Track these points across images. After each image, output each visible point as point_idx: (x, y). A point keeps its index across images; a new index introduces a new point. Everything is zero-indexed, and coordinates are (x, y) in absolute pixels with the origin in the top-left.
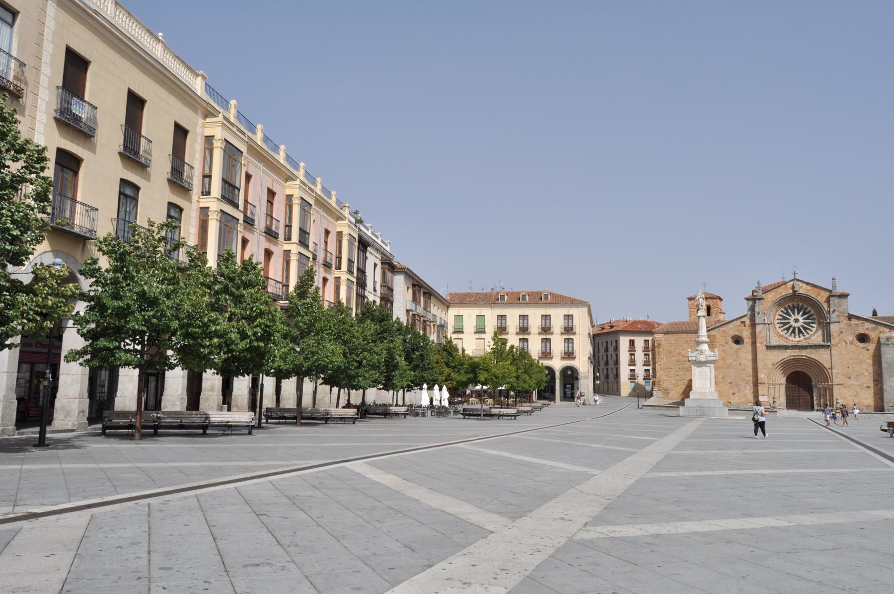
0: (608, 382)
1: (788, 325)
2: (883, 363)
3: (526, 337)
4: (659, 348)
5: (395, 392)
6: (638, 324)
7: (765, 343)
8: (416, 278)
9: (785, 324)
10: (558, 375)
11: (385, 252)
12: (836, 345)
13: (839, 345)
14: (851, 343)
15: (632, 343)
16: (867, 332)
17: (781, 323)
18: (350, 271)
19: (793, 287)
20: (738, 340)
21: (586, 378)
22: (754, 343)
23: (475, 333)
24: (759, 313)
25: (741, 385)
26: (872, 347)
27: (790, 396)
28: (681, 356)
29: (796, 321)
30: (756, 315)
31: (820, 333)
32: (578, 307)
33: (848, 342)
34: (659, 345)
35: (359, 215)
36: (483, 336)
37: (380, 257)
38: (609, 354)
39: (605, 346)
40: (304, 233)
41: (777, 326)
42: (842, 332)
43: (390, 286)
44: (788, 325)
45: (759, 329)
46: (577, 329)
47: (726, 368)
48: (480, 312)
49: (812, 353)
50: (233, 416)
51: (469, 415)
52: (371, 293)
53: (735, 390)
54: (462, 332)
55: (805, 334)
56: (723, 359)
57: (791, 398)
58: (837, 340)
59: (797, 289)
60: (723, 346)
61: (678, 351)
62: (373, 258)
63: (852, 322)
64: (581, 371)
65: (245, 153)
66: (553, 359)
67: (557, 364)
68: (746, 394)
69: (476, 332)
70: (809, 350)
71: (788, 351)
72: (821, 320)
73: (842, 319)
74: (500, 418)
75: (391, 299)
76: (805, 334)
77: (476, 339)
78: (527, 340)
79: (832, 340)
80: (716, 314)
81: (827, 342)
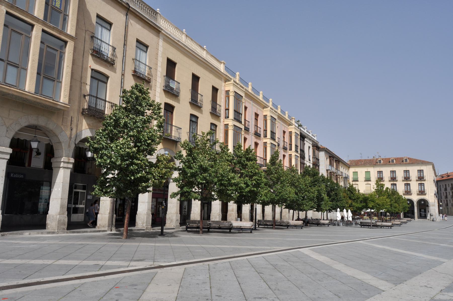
0: (448, 208)
3: (395, 183)
5: (323, 213)
8: (331, 153)
10: (415, 204)
11: (314, 140)
18: (296, 151)
21: (434, 205)
23: (365, 181)
32: (426, 165)
35: (300, 123)
36: (369, 182)
37: (311, 143)
38: (448, 192)
39: (444, 187)
40: (273, 133)
43: (317, 158)
46: (426, 178)
48: (367, 170)
50: (243, 224)
51: (364, 225)
52: (308, 162)
54: (357, 181)
62: (308, 144)
64: (430, 201)
65: (244, 97)
66: (412, 195)
67: (415, 198)
69: (365, 181)
74: (382, 227)
75: (318, 164)
77: (366, 184)
78: (395, 184)
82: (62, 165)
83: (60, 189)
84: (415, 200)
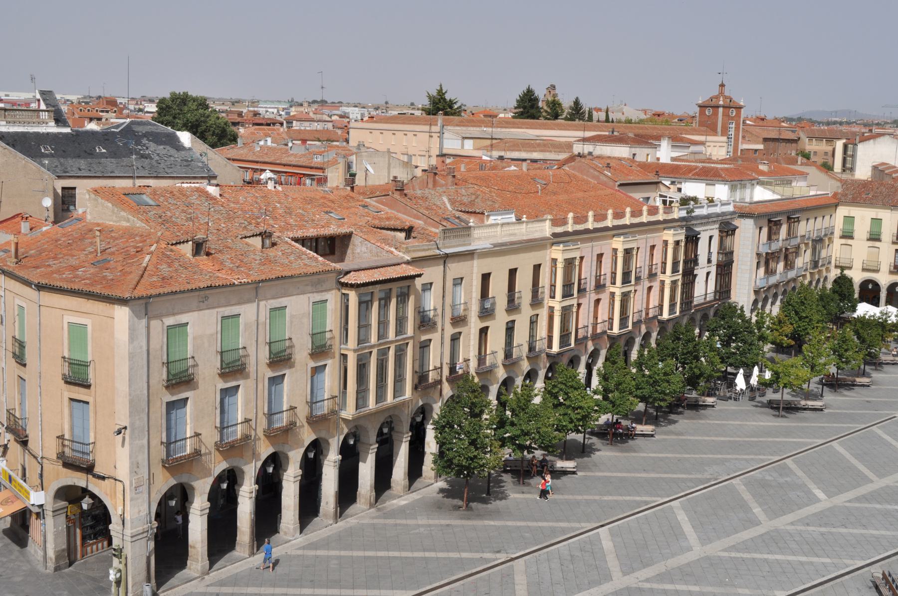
18: (675, 270)
23: (868, 240)
36: (877, 244)
48: (877, 215)
54: (851, 237)
69: (870, 239)
82: (404, 440)
83: (403, 460)
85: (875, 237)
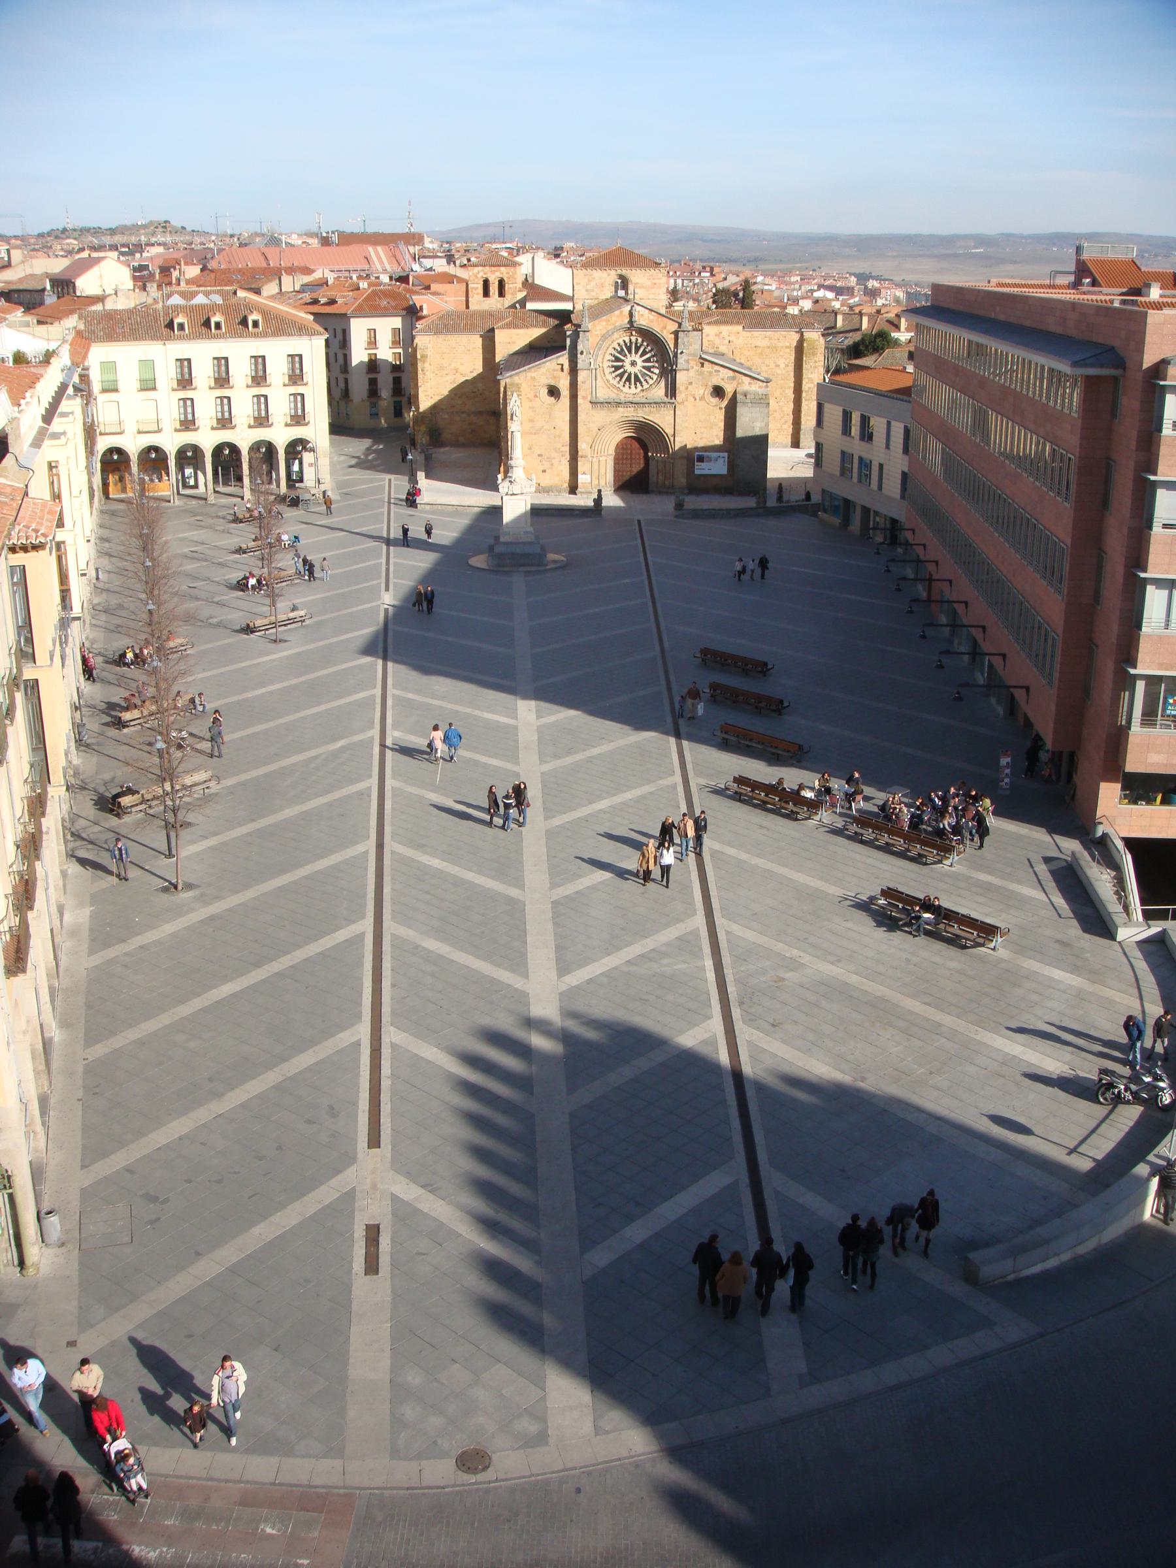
1: (622, 370)
2: (737, 429)
4: (424, 362)
6: (380, 298)
7: (589, 398)
9: (617, 368)
12: (683, 402)
13: (685, 403)
14: (702, 398)
15: (373, 332)
16: (722, 384)
17: (613, 366)
19: (631, 315)
20: (553, 392)
22: (574, 397)
23: (142, 390)
24: (582, 353)
25: (554, 458)
26: (725, 402)
27: (619, 471)
28: (458, 374)
29: (633, 364)
30: (579, 355)
31: (663, 383)
33: (697, 398)
34: (424, 357)
36: (152, 394)
41: (608, 371)
42: (691, 383)
44: (622, 370)
45: (582, 376)
47: (535, 434)
49: (650, 412)
53: (546, 466)
55: (644, 383)
56: (531, 421)
57: (621, 473)
58: (683, 395)
59: (637, 319)
60: (531, 401)
61: (453, 365)
63: (704, 369)
68: (562, 471)
70: (647, 409)
71: (620, 409)
72: (665, 365)
73: (692, 363)
76: (644, 383)
79: (677, 395)
80: (512, 294)
81: (671, 399)
84: (281, 444)
85: (148, 386)
